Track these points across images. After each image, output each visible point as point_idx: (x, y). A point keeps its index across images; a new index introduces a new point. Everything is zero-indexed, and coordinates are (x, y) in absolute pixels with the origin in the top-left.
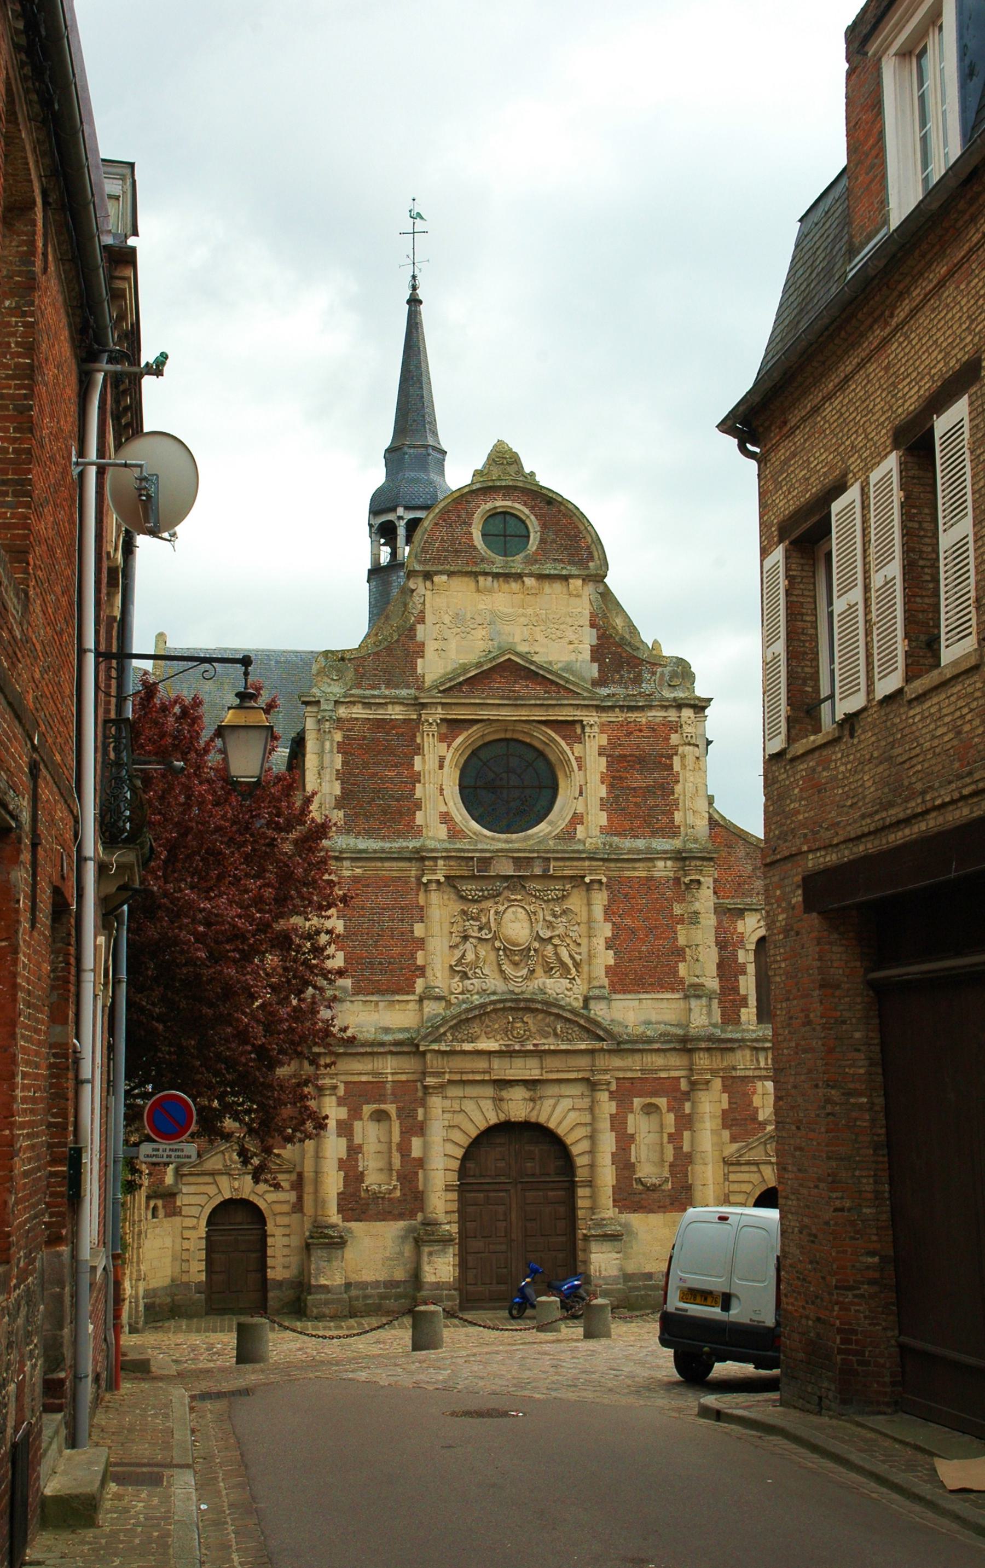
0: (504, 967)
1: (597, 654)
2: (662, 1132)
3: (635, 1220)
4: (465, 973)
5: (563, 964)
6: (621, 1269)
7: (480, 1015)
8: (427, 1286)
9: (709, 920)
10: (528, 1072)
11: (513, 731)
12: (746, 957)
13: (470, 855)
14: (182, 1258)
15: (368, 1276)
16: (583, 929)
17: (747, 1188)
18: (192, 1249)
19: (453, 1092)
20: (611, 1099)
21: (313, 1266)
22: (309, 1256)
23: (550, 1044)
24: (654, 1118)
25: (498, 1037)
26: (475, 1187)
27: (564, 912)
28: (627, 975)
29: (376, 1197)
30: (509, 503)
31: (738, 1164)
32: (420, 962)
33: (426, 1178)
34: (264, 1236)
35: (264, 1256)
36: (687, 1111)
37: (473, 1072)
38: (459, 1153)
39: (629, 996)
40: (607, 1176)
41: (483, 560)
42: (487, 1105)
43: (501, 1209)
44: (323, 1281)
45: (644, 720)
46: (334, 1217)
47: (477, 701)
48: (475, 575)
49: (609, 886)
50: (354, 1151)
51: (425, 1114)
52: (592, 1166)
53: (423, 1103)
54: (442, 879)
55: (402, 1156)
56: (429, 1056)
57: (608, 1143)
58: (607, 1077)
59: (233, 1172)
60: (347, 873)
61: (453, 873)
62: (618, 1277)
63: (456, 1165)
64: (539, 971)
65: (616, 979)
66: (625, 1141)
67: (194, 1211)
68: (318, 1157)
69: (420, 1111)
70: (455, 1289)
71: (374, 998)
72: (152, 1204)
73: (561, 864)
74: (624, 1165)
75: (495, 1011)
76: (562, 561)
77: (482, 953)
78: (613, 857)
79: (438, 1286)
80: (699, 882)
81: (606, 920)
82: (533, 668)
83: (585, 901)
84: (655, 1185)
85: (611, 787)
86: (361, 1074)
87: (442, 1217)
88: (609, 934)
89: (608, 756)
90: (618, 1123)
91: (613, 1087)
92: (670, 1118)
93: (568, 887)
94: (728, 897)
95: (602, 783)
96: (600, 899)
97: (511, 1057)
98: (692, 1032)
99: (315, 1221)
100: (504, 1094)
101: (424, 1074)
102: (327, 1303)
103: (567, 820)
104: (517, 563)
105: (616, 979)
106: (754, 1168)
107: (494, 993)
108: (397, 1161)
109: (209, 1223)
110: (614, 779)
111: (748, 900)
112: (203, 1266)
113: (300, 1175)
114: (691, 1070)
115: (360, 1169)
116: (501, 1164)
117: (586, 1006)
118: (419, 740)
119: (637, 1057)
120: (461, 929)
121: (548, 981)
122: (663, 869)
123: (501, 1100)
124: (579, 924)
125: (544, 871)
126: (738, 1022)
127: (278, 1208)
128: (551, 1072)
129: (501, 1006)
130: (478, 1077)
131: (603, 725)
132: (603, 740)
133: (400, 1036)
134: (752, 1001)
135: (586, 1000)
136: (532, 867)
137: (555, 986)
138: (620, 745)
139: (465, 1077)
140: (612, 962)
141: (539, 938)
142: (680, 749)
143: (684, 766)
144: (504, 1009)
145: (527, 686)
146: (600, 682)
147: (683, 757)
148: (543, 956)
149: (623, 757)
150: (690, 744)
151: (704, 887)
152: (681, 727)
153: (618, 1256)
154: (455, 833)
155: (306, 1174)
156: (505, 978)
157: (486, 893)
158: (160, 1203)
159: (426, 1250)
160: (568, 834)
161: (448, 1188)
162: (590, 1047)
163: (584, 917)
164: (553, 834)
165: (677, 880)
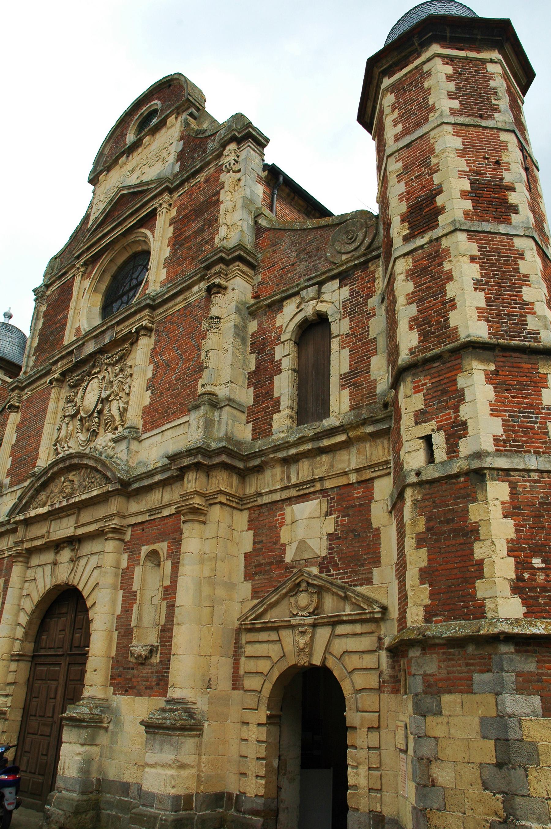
17: (264, 666)
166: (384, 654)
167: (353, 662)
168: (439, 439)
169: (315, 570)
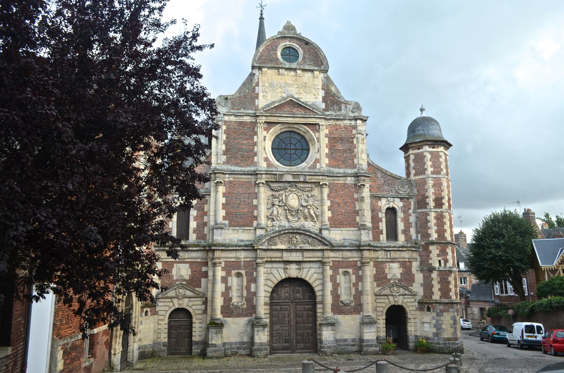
0: (289, 217)
1: (325, 100)
2: (350, 282)
3: (340, 318)
4: (273, 219)
5: (311, 216)
6: (335, 338)
7: (279, 235)
8: (256, 344)
9: (368, 200)
10: (298, 258)
11: (293, 127)
12: (382, 215)
13: (275, 173)
14: (157, 332)
15: (233, 340)
16: (319, 203)
17: (384, 305)
18: (162, 328)
19: (269, 265)
20: (330, 269)
21: (210, 336)
22: (209, 331)
23: (307, 247)
24: (347, 277)
25: (286, 244)
26: (276, 304)
27: (312, 196)
28: (336, 221)
29: (236, 307)
30: (291, 43)
31: (380, 295)
32: (255, 214)
33: (257, 300)
34: (191, 323)
35: (191, 331)
36: (360, 274)
37: (276, 258)
38: (270, 290)
39: (337, 229)
40: (329, 300)
41: (281, 64)
42: (281, 271)
43: (287, 312)
44: (214, 342)
45: (342, 125)
46: (219, 315)
47: (279, 115)
48: (278, 68)
49: (329, 187)
50: (228, 289)
51: (257, 274)
52: (323, 296)
53: (256, 270)
54: (264, 182)
55: (247, 291)
56: (258, 251)
57: (329, 286)
58: (329, 260)
59: (179, 297)
60: (227, 180)
61: (268, 180)
62: (334, 341)
63: (269, 295)
64: (302, 219)
65: (332, 222)
66: (336, 286)
67: (163, 313)
68: (213, 291)
69: (255, 273)
70: (268, 345)
71: (237, 228)
72: (145, 310)
73: (311, 177)
74: (336, 295)
75: (285, 233)
76: (311, 65)
77: (280, 211)
78: (331, 175)
79: (261, 344)
80: (364, 185)
81: (328, 199)
82: (300, 103)
83: (320, 192)
84: (348, 304)
85: (330, 149)
86: (231, 258)
87: (263, 316)
88: (329, 205)
89: (329, 138)
90: (333, 279)
91: (331, 264)
92: (353, 277)
93: (313, 186)
94: (375, 192)
95: (327, 147)
96: (326, 191)
97: (291, 252)
98: (362, 244)
99: (212, 317)
100: (288, 266)
101: (256, 258)
102: (215, 351)
103: (313, 161)
104: (294, 66)
105: (332, 222)
106: (386, 297)
107: (285, 227)
108: (245, 293)
109: (170, 318)
110: (331, 146)
111: (382, 193)
112: (166, 335)
113: (206, 299)
114: (362, 258)
115: (230, 296)
116: (287, 295)
117: (320, 232)
118: (256, 130)
119: (340, 253)
120: (271, 202)
121: (305, 222)
122: (350, 180)
123: (287, 269)
124: (317, 201)
125: (304, 180)
126: (379, 240)
127: (197, 312)
128: (307, 258)
129: (286, 231)
130: (278, 260)
131: (327, 126)
132: (327, 131)
133: (247, 243)
134: (385, 232)
135: (321, 230)
136: (299, 178)
137: (309, 225)
138: (333, 133)
139: (273, 260)
140: (330, 216)
141: (302, 206)
142: (356, 136)
143: (358, 142)
144: (288, 233)
145: (298, 110)
146: (326, 109)
147: (358, 138)
148: (304, 213)
149: (334, 138)
150: (360, 134)
151: (366, 187)
152: (357, 127)
153: (333, 332)
154: (269, 165)
155: (208, 298)
156: (289, 221)
157: (281, 188)
158: (149, 309)
159: (256, 329)
160: (314, 166)
161: (266, 304)
162: (322, 248)
163: (319, 197)
164: (308, 166)
165: (355, 185)
166: (416, 303)
167: (409, 304)
168: (442, 262)
169: (397, 281)
